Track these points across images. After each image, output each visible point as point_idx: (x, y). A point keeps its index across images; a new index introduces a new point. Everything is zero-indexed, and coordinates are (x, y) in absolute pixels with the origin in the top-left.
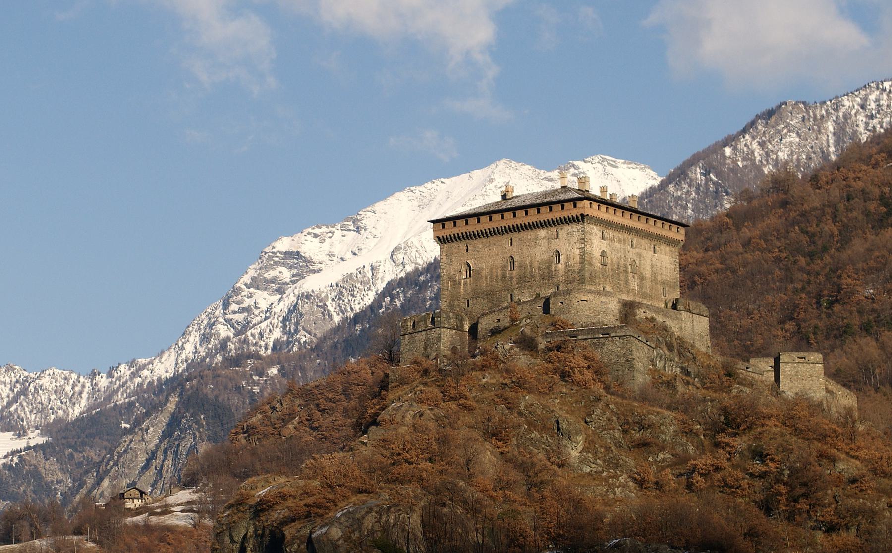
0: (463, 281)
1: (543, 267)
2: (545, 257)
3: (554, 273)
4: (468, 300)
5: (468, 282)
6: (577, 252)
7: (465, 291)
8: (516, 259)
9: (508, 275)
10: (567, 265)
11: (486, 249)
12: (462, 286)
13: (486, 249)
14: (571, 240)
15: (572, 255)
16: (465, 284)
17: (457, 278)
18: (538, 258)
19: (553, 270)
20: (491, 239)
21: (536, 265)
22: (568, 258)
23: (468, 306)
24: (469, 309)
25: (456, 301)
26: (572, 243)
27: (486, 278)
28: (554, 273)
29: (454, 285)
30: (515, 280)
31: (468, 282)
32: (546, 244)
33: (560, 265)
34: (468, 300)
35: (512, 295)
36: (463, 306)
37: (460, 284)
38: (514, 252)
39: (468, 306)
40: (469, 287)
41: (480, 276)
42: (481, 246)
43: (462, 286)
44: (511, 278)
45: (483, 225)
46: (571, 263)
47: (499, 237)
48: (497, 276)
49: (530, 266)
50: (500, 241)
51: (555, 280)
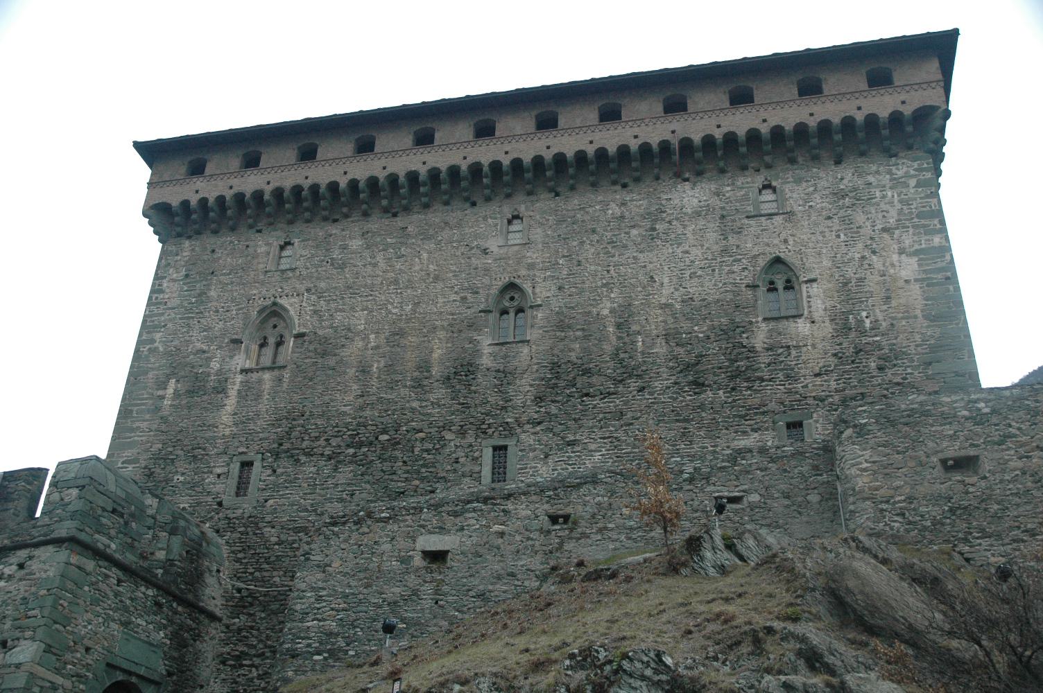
0: (239, 378)
1: (700, 330)
2: (707, 288)
3: (764, 359)
4: (246, 465)
5: (267, 386)
6: (909, 268)
7: (241, 421)
8: (541, 290)
9: (486, 361)
10: (843, 325)
11: (380, 257)
12: (231, 403)
13: (380, 257)
14: (860, 218)
15: (872, 281)
16: (249, 393)
17: (215, 365)
18: (666, 292)
19: (759, 346)
20: (413, 222)
21: (655, 321)
22: (848, 291)
23: (242, 488)
24: (246, 506)
25: (181, 466)
26: (867, 230)
27: (364, 370)
28: (764, 359)
29: (191, 393)
30: (524, 389)
31: (267, 386)
32: (712, 236)
33: (802, 327)
34: (246, 465)
35: (500, 450)
36: (219, 488)
37: (221, 390)
38: (531, 266)
39: (242, 488)
40: (264, 405)
41: (332, 362)
42: (356, 244)
43: (231, 403)
44: (505, 376)
45: (383, 162)
46: (871, 314)
47: (456, 213)
48: (424, 366)
49: (619, 326)
50: (459, 225)
51: (774, 392)
